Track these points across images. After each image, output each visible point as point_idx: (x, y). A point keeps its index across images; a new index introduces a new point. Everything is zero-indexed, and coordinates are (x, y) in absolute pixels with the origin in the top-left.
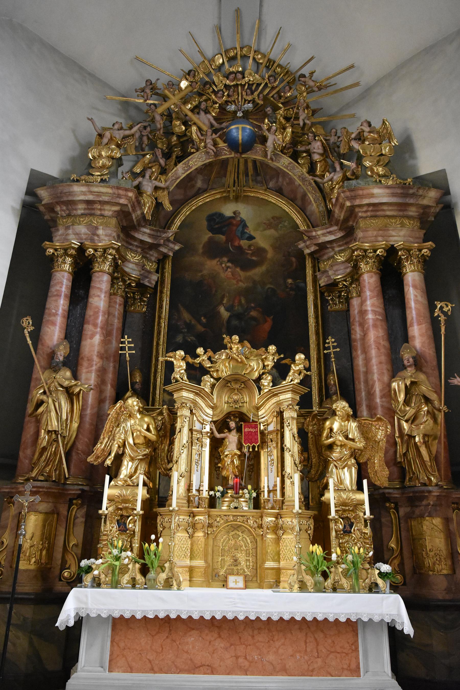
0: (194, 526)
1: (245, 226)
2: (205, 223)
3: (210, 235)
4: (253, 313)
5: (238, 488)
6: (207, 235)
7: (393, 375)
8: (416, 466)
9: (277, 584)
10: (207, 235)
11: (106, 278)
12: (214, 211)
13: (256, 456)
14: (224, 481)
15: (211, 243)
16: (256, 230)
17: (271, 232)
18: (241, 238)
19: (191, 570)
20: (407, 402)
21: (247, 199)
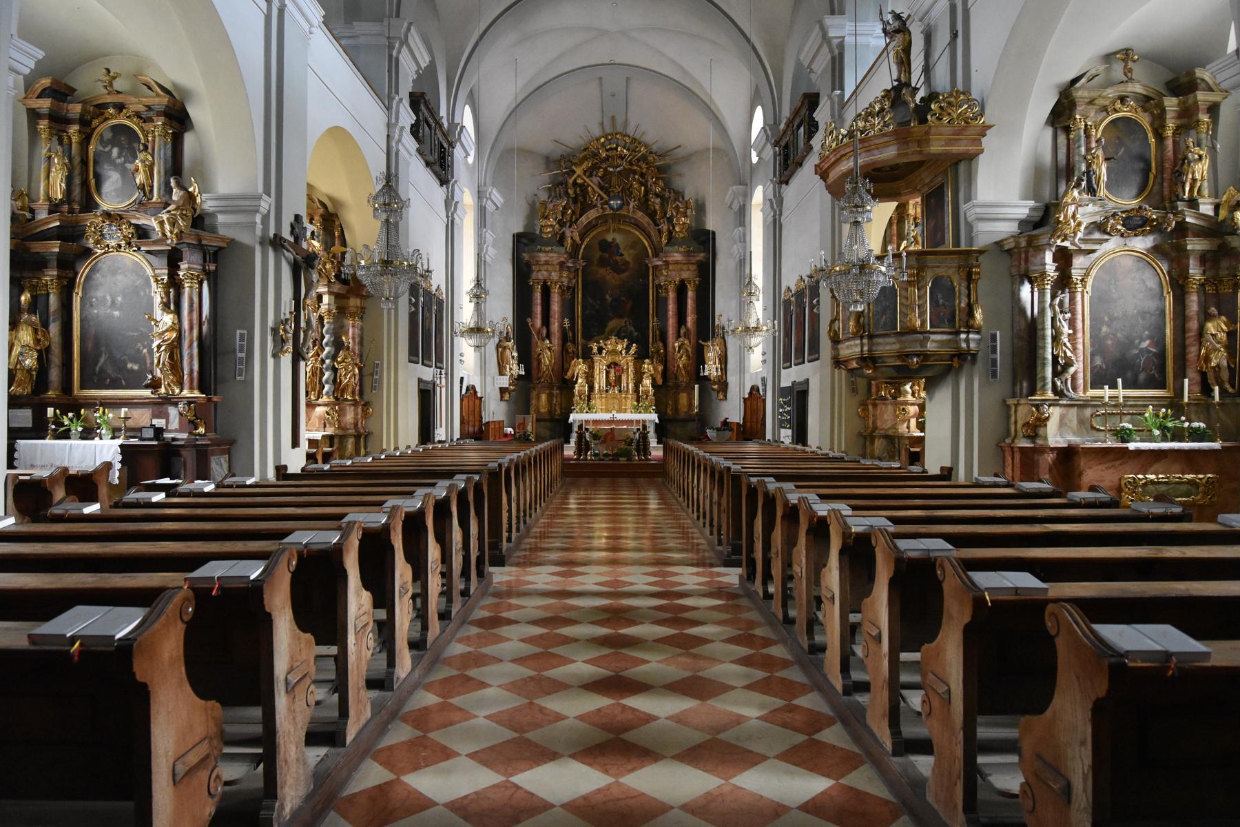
0: (602, 397)
1: (619, 248)
2: (597, 246)
3: (600, 253)
4: (623, 298)
5: (614, 387)
6: (598, 254)
7: (677, 340)
8: (679, 374)
9: (625, 412)
10: (598, 254)
11: (556, 295)
12: (600, 239)
13: (620, 377)
14: (610, 385)
15: (601, 258)
16: (624, 250)
17: (632, 251)
18: (617, 255)
19: (601, 409)
20: (679, 351)
21: (620, 231)
